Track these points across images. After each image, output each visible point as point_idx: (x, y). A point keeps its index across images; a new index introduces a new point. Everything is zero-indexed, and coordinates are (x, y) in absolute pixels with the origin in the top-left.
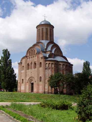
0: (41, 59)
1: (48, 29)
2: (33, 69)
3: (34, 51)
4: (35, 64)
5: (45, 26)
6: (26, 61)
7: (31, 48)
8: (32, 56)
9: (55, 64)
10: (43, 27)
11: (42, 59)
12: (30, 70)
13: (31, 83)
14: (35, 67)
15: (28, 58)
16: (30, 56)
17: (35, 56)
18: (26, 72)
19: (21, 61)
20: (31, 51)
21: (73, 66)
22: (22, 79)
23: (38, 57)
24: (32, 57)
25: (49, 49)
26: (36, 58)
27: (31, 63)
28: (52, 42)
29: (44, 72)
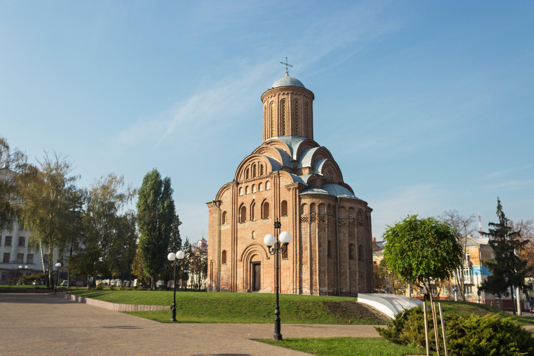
0: (286, 190)
1: (299, 102)
2: (259, 222)
3: (262, 165)
4: (265, 205)
5: (290, 92)
7: (251, 157)
8: (254, 182)
9: (329, 205)
10: (285, 96)
11: (289, 189)
12: (248, 223)
13: (251, 262)
14: (265, 215)
15: (241, 188)
18: (235, 231)
19: (218, 195)
21: (372, 213)
22: (222, 251)
23: (277, 186)
24: (253, 185)
25: (306, 162)
27: (253, 204)
28: (309, 143)
29: (298, 231)
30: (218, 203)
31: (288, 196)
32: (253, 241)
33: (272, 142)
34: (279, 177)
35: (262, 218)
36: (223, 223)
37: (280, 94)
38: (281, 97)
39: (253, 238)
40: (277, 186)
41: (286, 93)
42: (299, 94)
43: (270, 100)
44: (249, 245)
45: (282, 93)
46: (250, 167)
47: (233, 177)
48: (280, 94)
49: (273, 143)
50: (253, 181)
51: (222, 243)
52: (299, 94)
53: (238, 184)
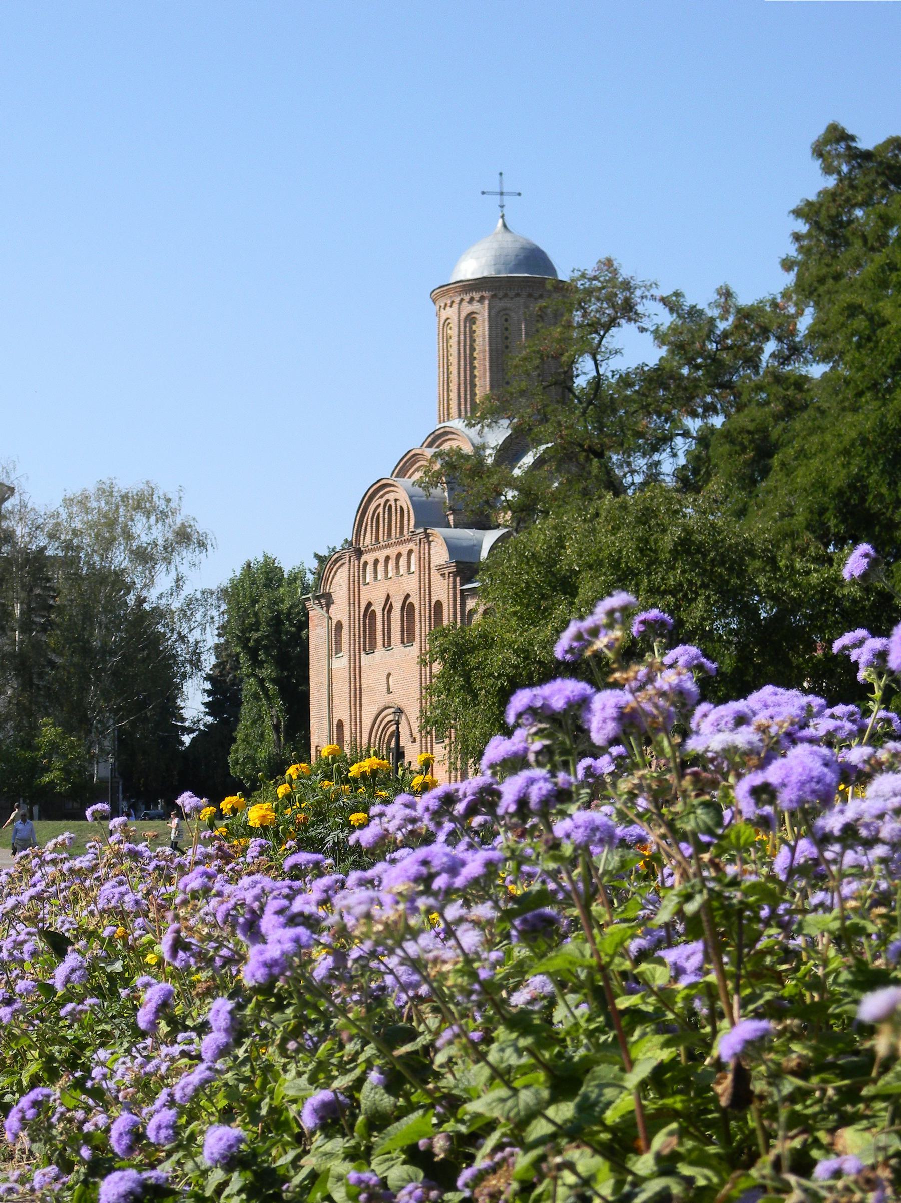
5: (486, 294)
6: (356, 585)
7: (381, 487)
8: (387, 552)
10: (476, 306)
11: (443, 575)
15: (366, 563)
16: (380, 548)
17: (404, 549)
18: (356, 673)
20: (381, 509)
22: (335, 722)
23: (425, 566)
24: (388, 558)
26: (413, 569)
27: (388, 607)
30: (323, 601)
31: (442, 590)
32: (385, 700)
33: (446, 433)
34: (430, 542)
35: (403, 642)
36: (339, 650)
37: (462, 300)
38: (467, 308)
39: (389, 689)
40: (425, 566)
41: (476, 296)
42: (511, 294)
43: (444, 314)
44: (381, 707)
45: (467, 298)
46: (381, 509)
47: (348, 533)
48: (462, 300)
49: (450, 437)
50: (387, 546)
51: (336, 702)
52: (511, 294)
53: (359, 553)
